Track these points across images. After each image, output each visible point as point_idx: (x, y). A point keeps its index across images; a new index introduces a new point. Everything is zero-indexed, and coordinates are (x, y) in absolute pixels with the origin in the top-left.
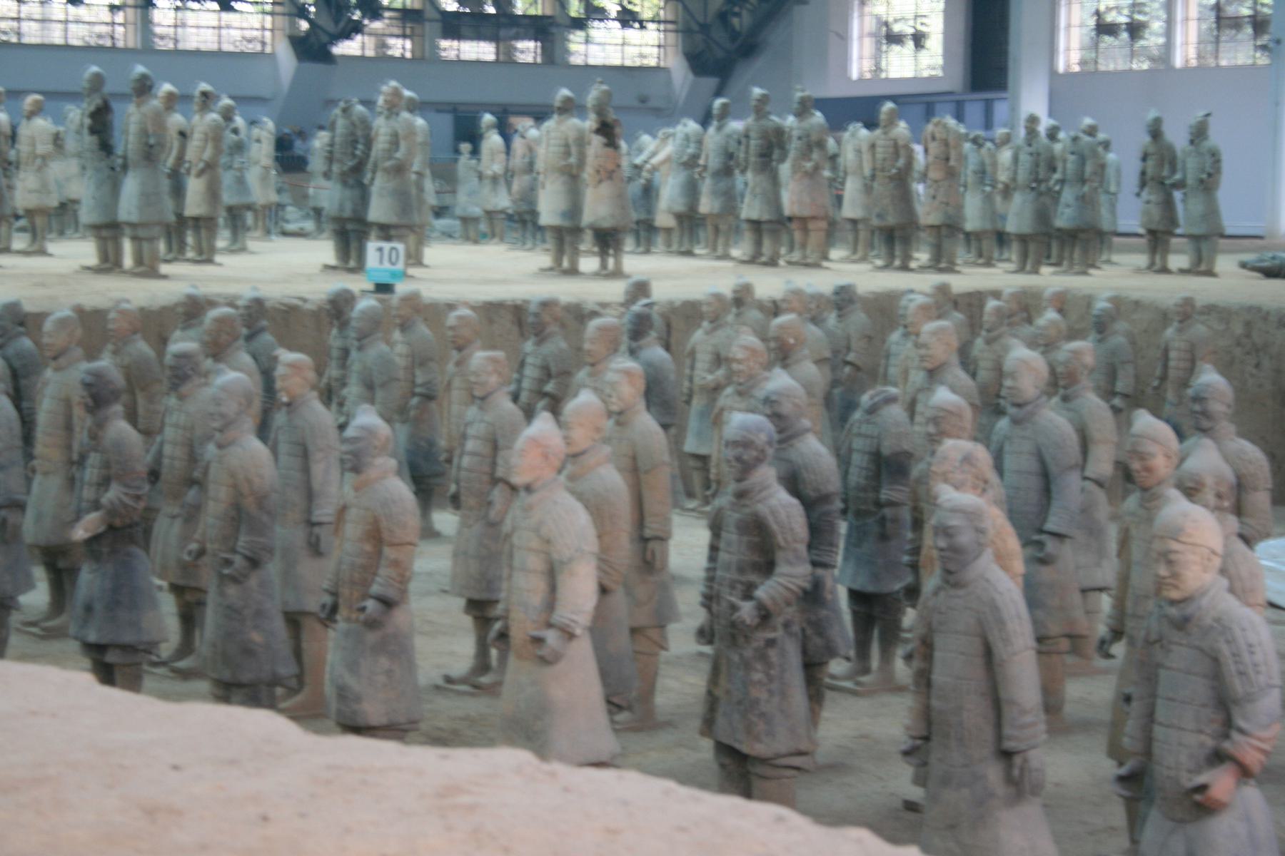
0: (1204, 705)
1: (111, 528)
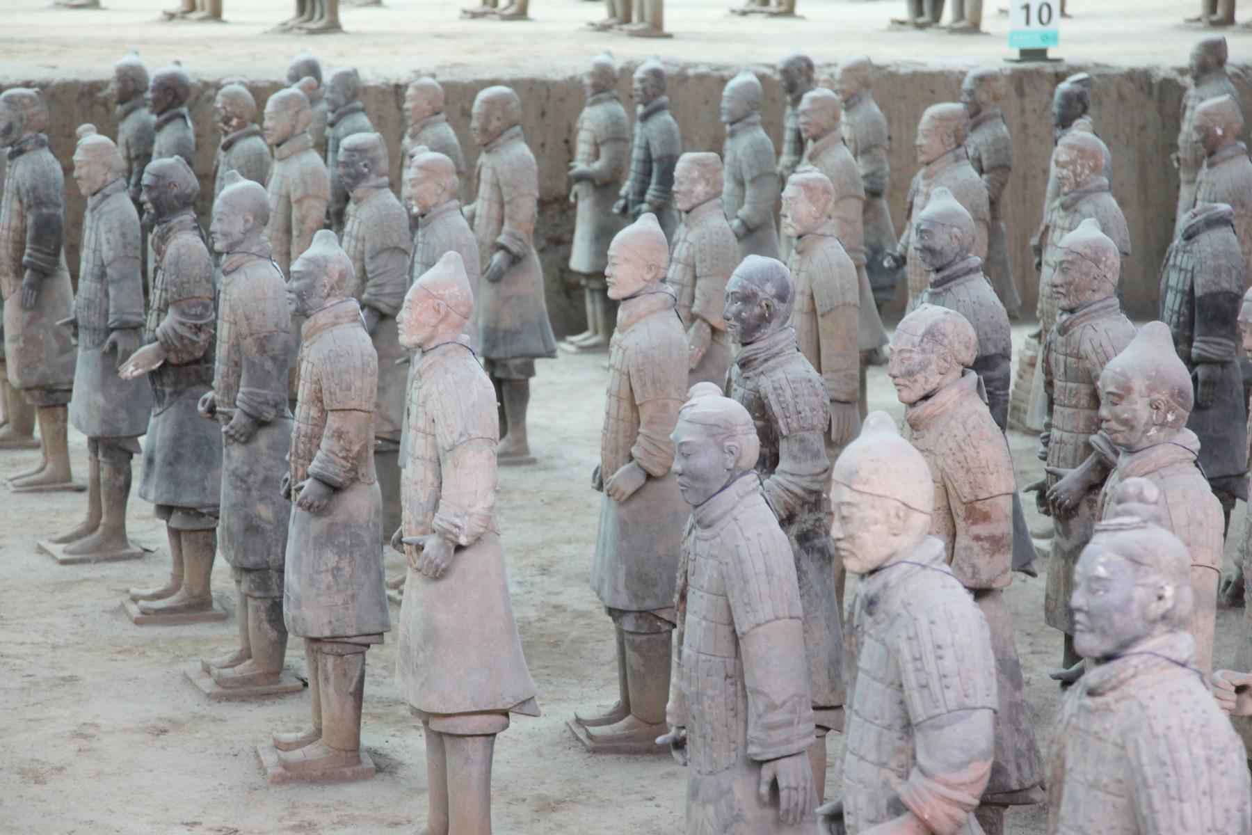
0: (889, 727)
1: (166, 364)
